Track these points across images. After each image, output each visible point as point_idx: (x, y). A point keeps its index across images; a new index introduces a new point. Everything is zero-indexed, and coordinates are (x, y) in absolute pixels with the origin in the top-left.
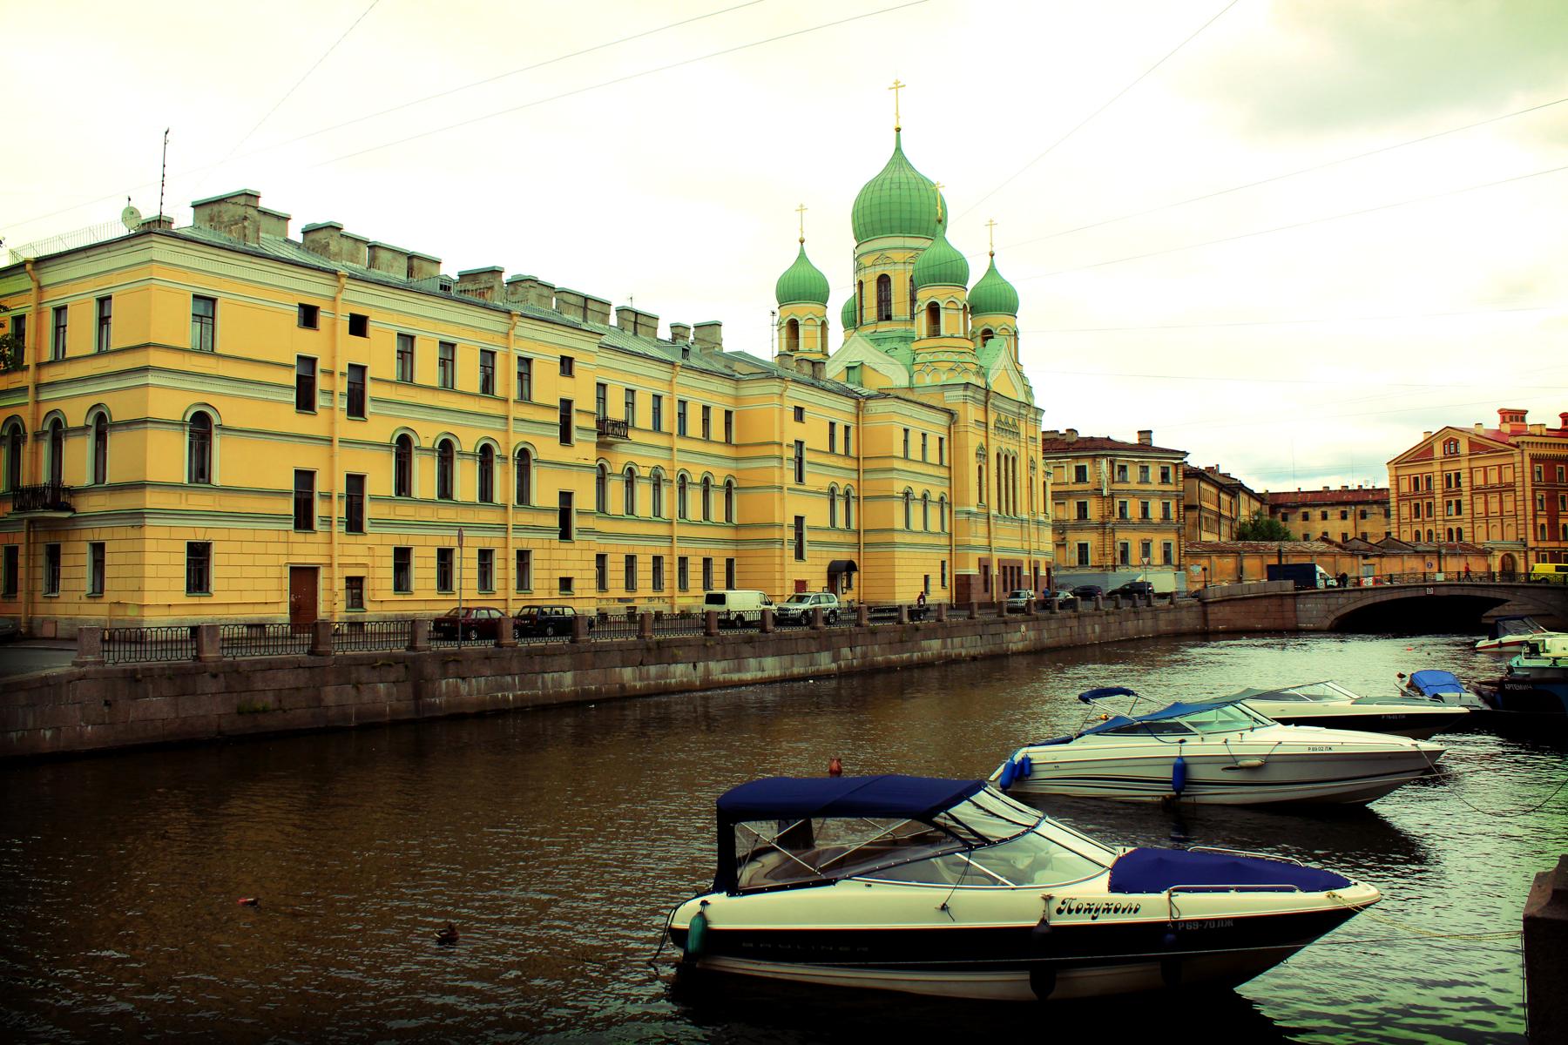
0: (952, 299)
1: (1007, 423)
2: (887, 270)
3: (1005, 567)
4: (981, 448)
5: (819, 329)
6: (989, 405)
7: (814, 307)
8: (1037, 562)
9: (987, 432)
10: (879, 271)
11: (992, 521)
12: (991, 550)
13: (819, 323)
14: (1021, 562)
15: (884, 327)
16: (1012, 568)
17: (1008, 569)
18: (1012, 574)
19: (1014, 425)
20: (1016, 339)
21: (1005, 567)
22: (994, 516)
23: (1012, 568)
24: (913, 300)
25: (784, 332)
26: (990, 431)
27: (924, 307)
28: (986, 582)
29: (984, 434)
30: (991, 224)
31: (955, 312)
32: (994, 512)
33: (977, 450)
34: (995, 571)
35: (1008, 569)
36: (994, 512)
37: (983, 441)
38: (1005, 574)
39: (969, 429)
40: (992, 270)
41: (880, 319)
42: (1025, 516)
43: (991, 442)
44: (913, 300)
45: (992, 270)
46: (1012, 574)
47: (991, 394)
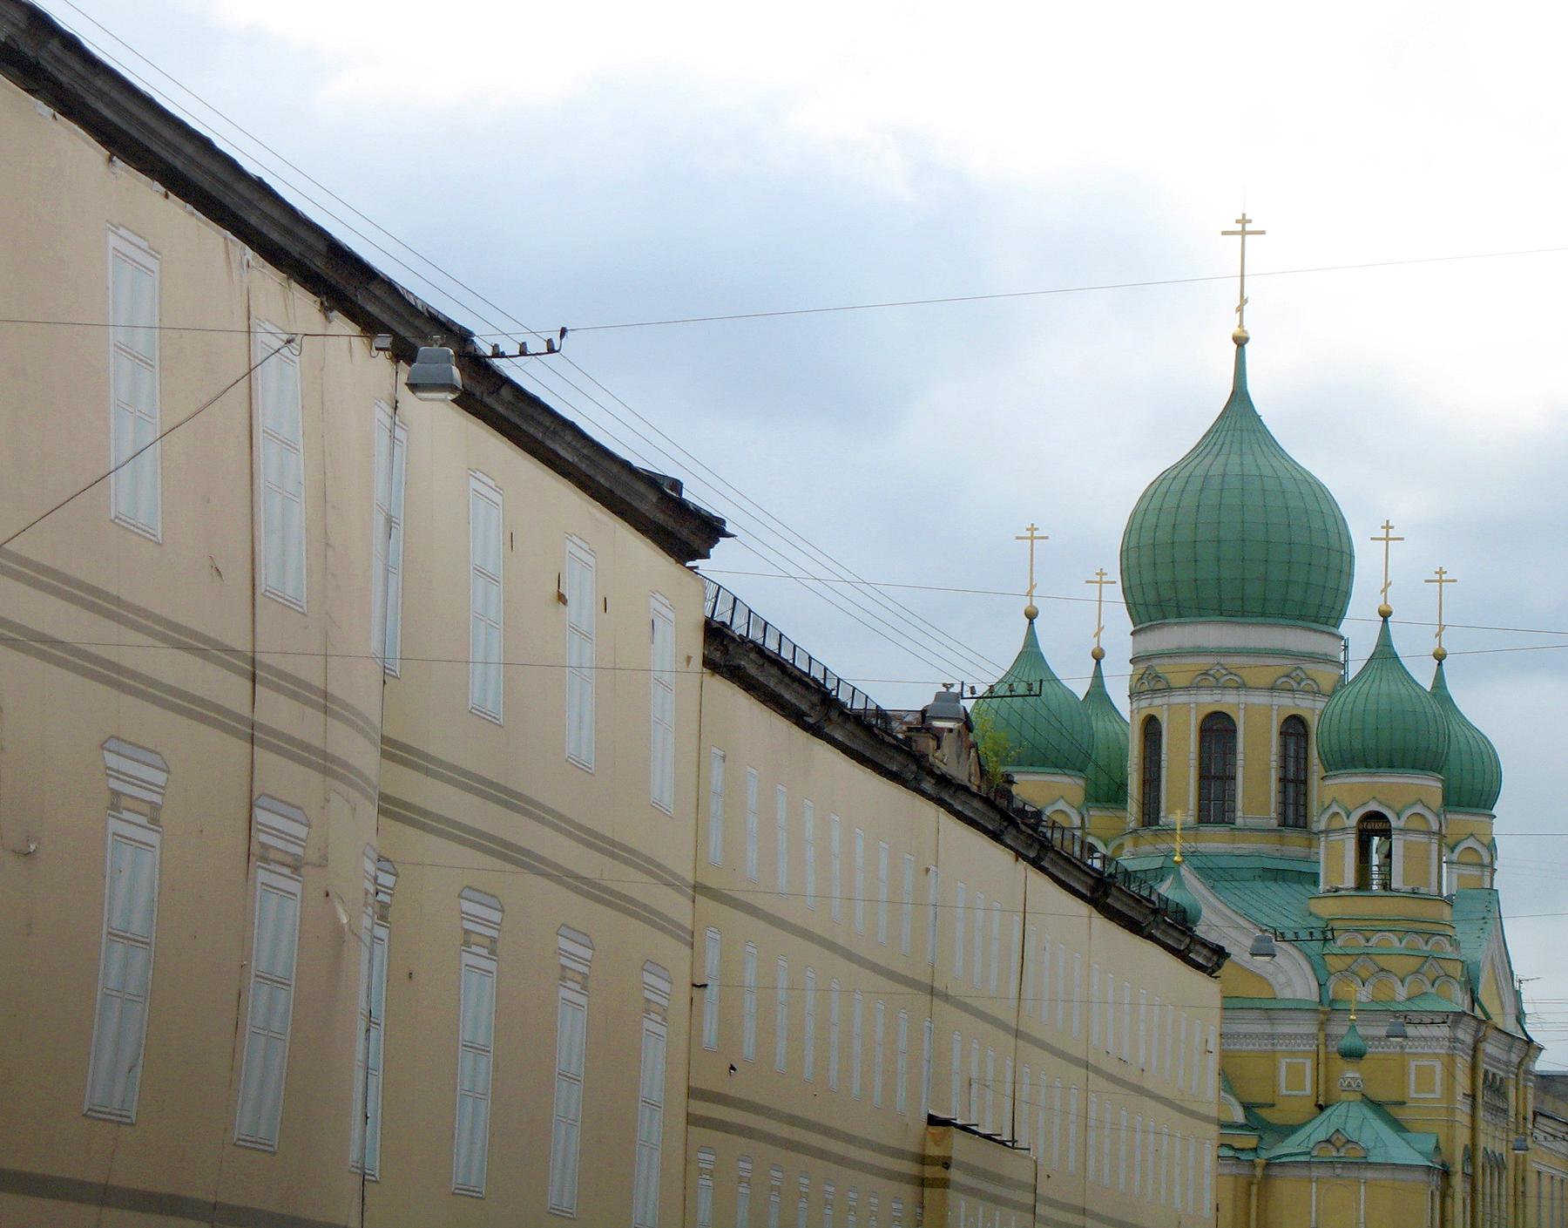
0: (1418, 809)
2: (1227, 701)
10: (1210, 701)
15: (1215, 842)
41: (1203, 818)
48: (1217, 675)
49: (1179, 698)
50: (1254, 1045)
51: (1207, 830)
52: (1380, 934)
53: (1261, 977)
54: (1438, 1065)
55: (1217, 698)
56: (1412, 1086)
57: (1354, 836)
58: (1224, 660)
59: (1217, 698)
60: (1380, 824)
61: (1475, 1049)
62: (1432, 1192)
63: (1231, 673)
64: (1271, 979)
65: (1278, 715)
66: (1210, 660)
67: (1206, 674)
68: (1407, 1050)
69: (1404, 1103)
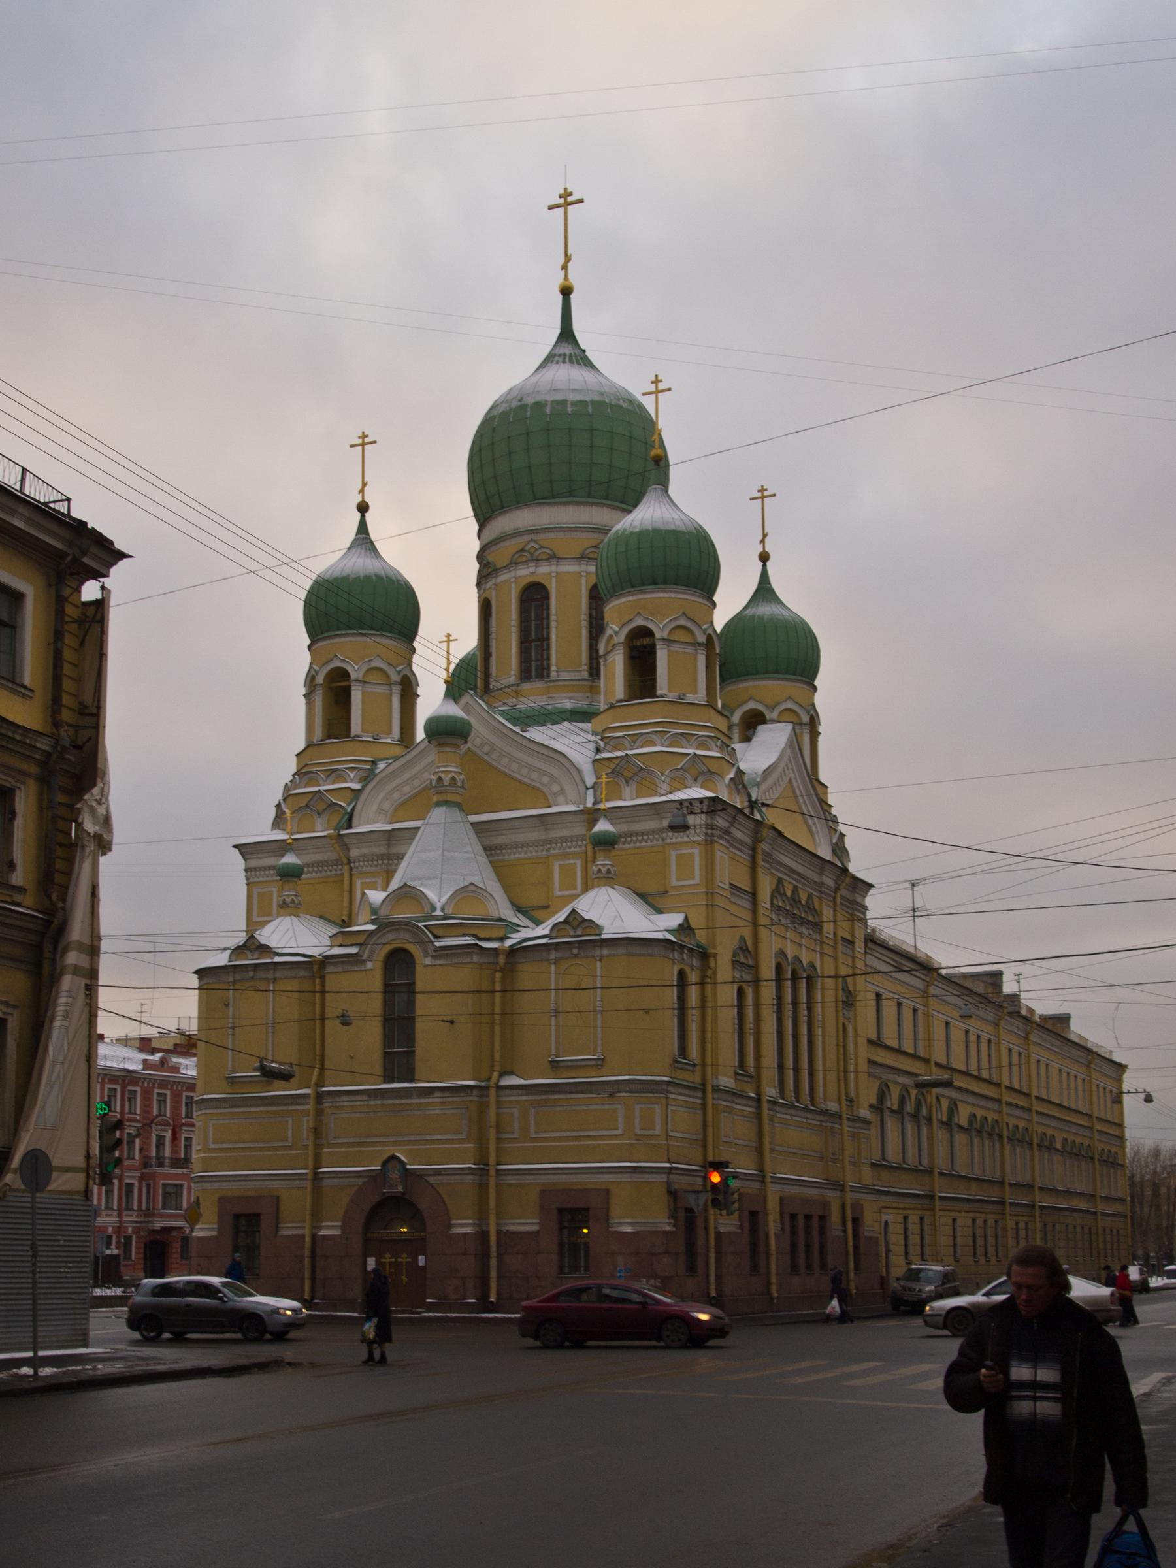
0: (683, 622)
1: (795, 900)
2: (542, 572)
3: (793, 1216)
4: (743, 948)
5: (397, 689)
6: (760, 857)
7: (379, 646)
8: (858, 1207)
9: (754, 912)
10: (526, 573)
11: (766, 1112)
12: (763, 1182)
13: (395, 678)
14: (825, 1205)
16: (808, 1217)
17: (801, 1221)
18: (808, 1232)
19: (810, 908)
20: (815, 735)
21: (793, 1216)
22: (773, 1103)
23: (808, 1217)
24: (596, 627)
25: (318, 699)
26: (761, 911)
27: (621, 638)
28: (754, 1248)
29: (747, 915)
30: (763, 495)
31: (689, 650)
32: (770, 1091)
33: (735, 954)
34: (772, 1223)
35: (801, 1221)
36: (770, 1091)
37: (747, 933)
38: (794, 1232)
39: (719, 901)
40: (764, 591)
41: (526, 674)
42: (832, 1106)
43: (763, 933)
44: (596, 627)
45: (764, 591)
46: (808, 1232)
47: (765, 832)
48: (532, 550)
49: (504, 577)
50: (531, 852)
51: (526, 686)
52: (644, 736)
53: (537, 789)
54: (696, 852)
55: (532, 569)
56: (674, 877)
57: (622, 651)
58: (535, 537)
59: (532, 569)
60: (648, 639)
61: (754, 849)
62: (682, 974)
63: (542, 547)
64: (544, 789)
65: (586, 581)
66: (526, 538)
67: (522, 550)
68: (668, 841)
69: (667, 892)
